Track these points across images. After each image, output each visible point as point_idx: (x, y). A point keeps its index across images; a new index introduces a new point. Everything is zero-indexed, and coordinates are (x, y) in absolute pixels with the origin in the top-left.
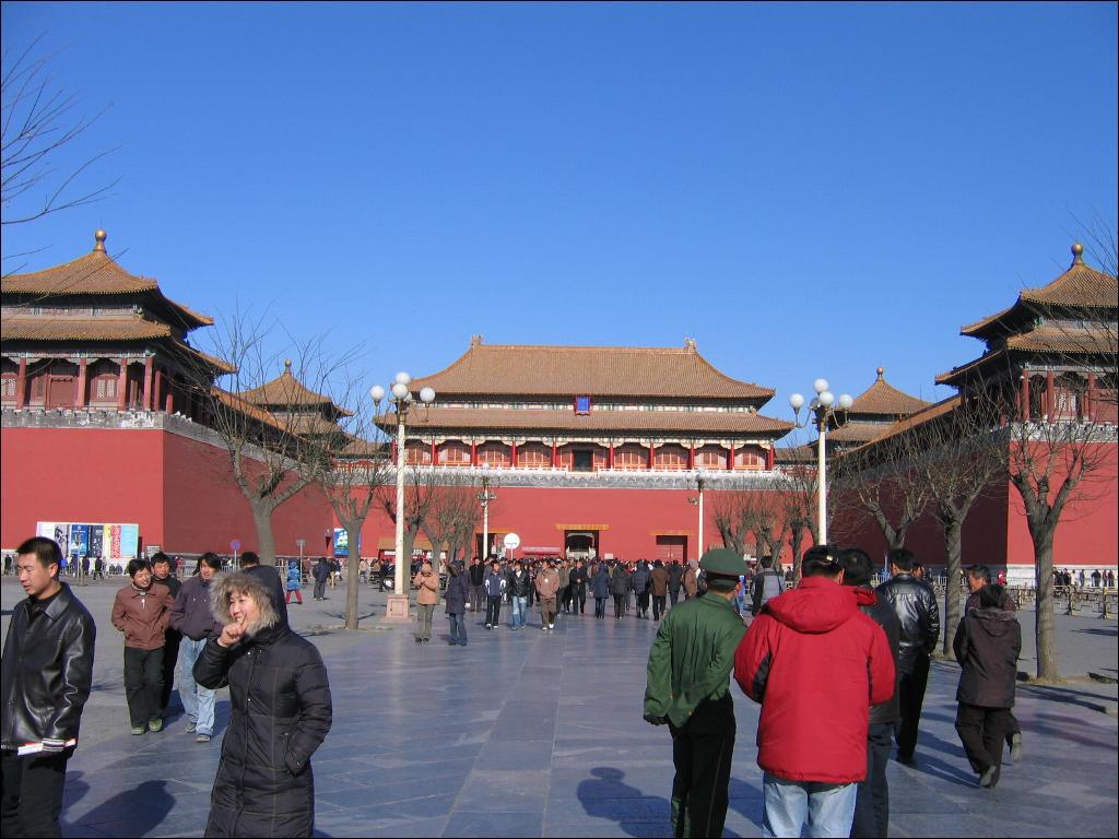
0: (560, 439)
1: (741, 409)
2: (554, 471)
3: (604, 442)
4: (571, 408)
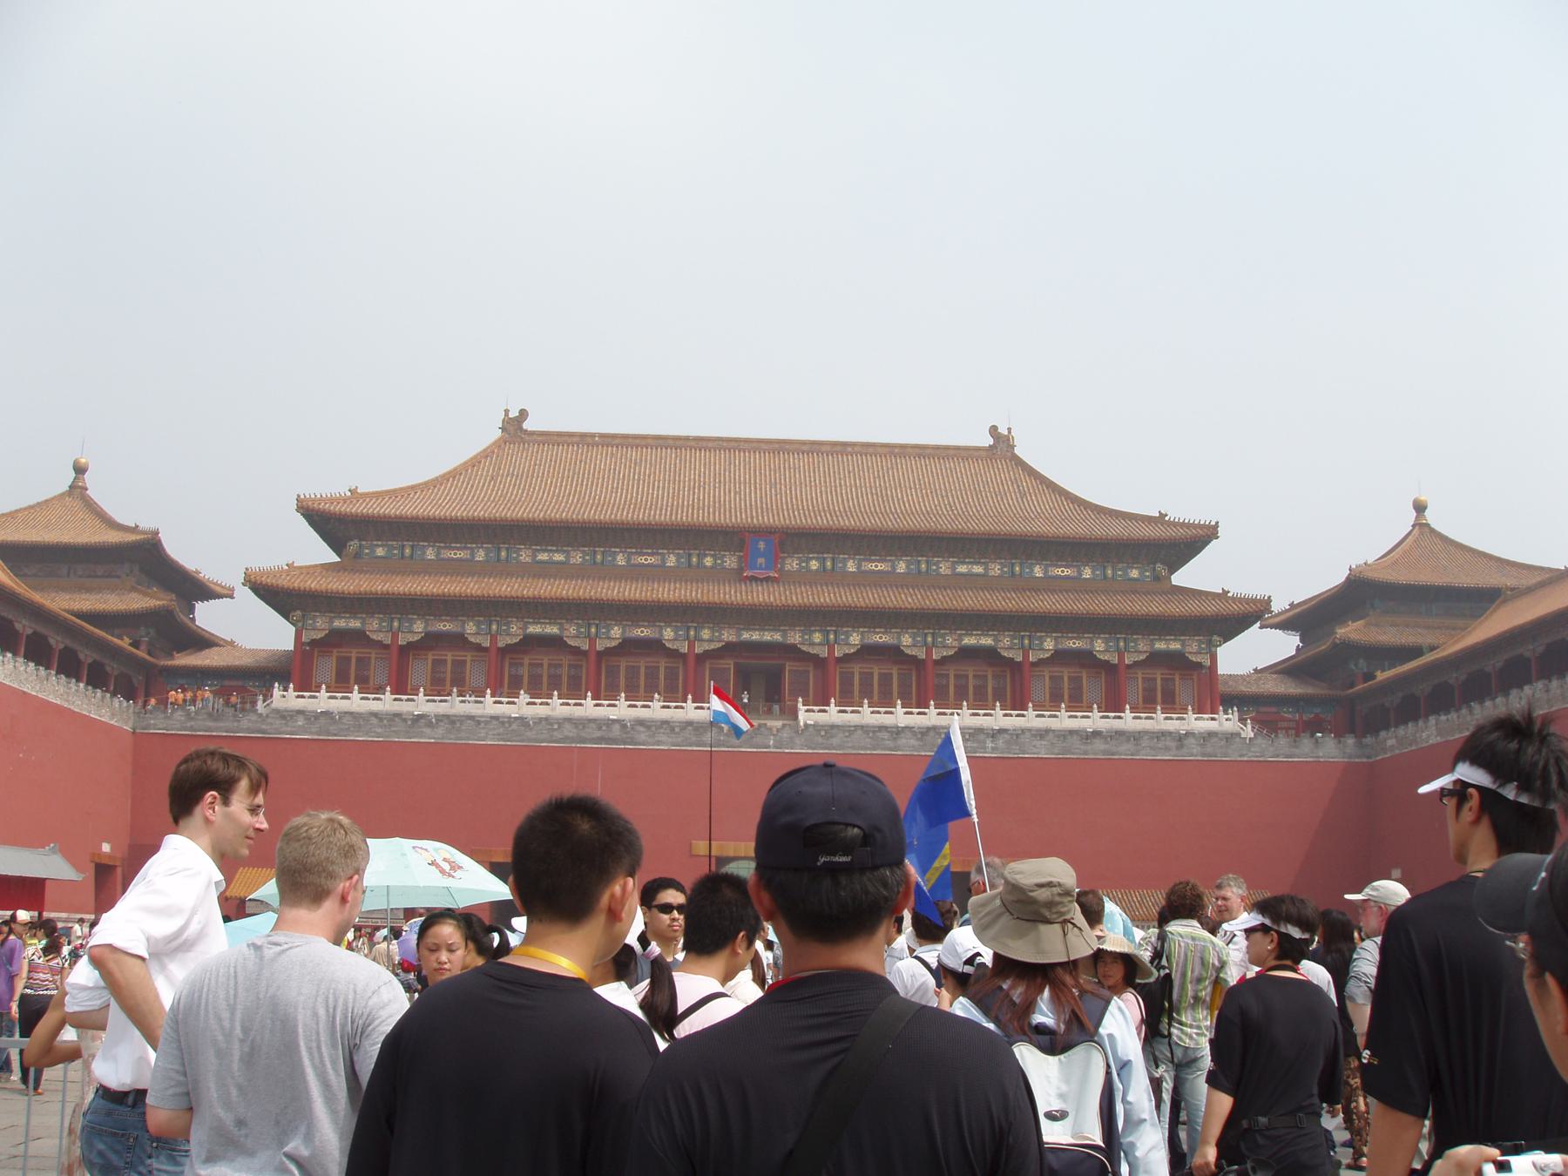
1: (1134, 574)
4: (730, 561)
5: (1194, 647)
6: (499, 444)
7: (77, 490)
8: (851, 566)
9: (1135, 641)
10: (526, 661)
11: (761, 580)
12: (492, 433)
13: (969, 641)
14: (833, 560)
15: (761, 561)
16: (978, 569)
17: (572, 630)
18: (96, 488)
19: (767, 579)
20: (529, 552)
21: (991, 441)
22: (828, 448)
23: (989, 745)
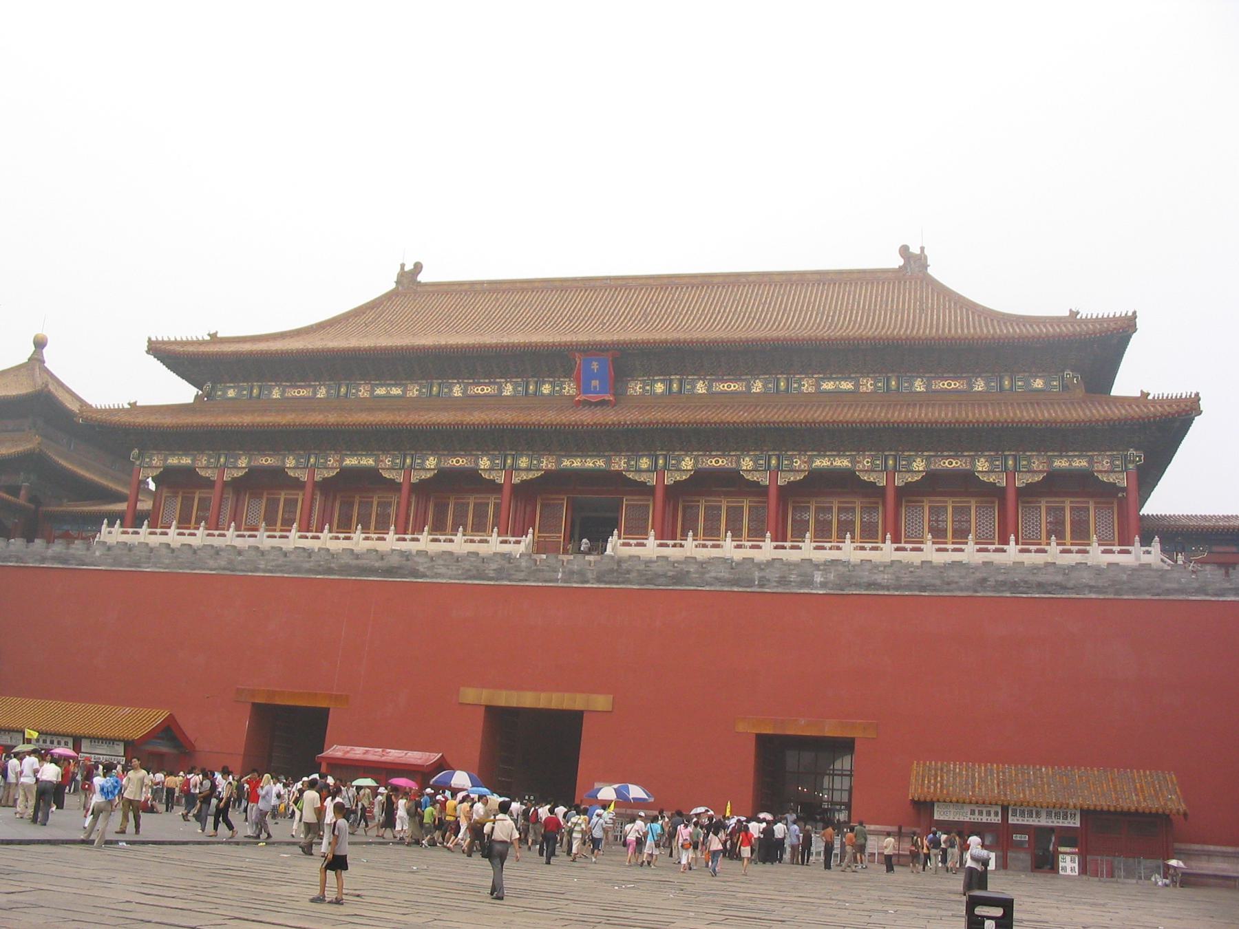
0: (523, 462)
1: (1038, 384)
2: (494, 544)
3: (642, 468)
4: (569, 389)
5: (1106, 465)
6: (389, 296)
7: (36, 360)
8: (701, 388)
9: (1029, 458)
10: (357, 499)
11: (597, 404)
12: (388, 284)
13: (821, 463)
14: (680, 382)
15: (595, 383)
16: (847, 386)
17: (388, 462)
18: (53, 360)
19: (603, 403)
20: (368, 387)
21: (897, 262)
22: (721, 279)
23: (818, 578)
